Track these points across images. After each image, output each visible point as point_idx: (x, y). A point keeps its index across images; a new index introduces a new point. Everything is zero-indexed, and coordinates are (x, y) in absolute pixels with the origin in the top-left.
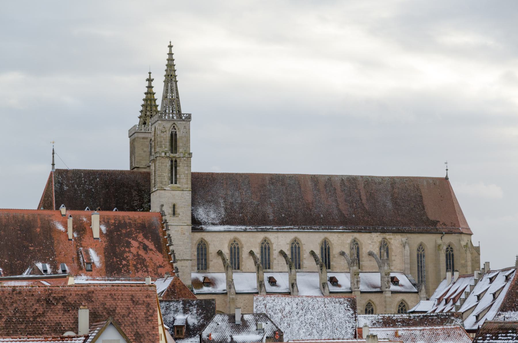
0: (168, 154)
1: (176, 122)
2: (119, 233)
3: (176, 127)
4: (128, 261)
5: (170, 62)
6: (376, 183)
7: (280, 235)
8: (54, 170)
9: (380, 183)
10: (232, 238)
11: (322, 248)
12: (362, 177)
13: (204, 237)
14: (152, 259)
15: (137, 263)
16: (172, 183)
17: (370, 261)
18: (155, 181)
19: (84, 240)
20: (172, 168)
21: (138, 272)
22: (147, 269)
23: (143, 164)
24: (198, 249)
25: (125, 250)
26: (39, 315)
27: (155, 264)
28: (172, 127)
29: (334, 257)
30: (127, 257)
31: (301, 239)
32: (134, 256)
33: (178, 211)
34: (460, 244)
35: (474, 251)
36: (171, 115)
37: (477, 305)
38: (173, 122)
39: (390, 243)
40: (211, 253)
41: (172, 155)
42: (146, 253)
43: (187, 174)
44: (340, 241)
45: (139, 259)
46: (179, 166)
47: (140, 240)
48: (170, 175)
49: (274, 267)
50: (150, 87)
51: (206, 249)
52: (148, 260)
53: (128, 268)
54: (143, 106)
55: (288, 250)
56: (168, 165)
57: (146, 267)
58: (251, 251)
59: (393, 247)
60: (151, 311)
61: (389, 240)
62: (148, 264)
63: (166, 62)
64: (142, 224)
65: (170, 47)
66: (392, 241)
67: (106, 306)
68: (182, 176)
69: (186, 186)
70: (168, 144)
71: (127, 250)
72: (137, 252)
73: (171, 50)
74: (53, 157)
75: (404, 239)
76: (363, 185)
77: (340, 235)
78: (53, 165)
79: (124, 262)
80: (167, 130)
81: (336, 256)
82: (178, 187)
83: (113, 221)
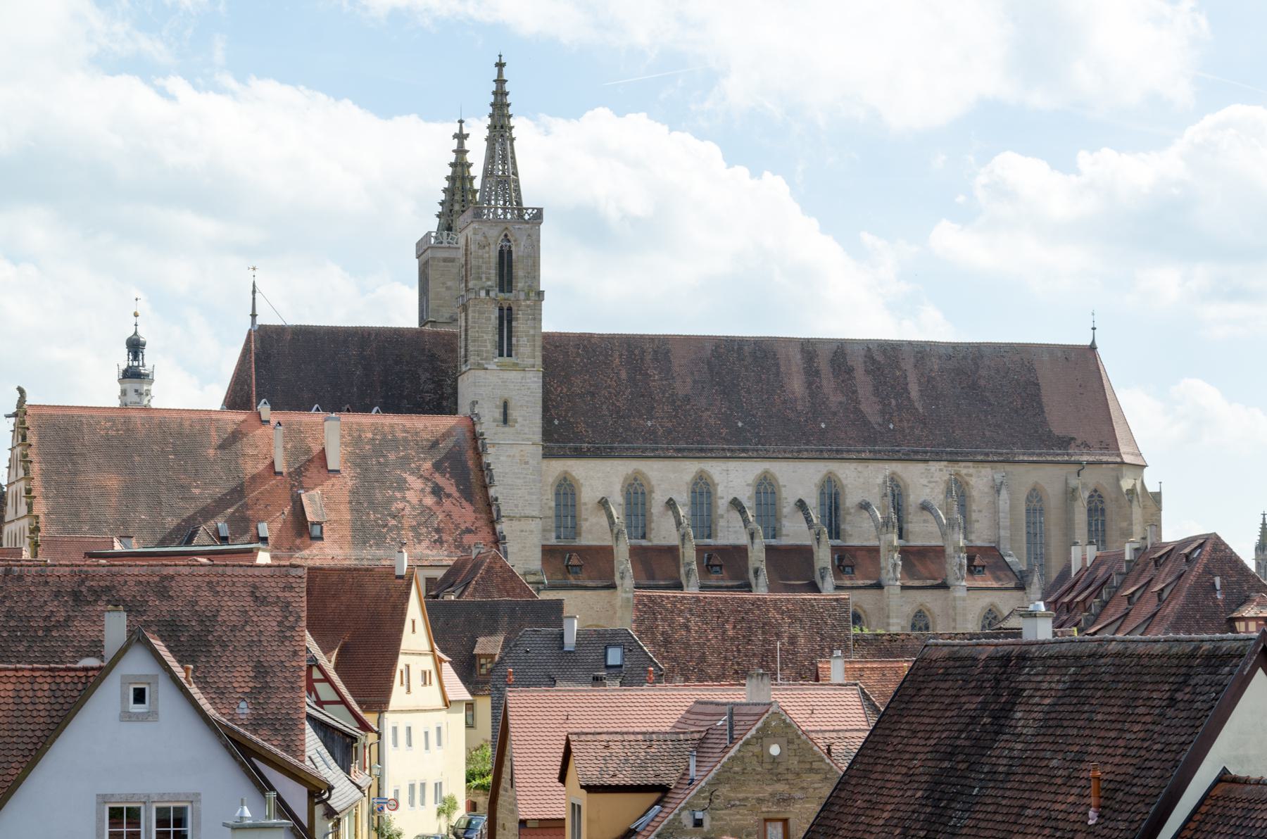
0: (492, 294)
2: (382, 460)
7: (732, 465)
9: (950, 358)
11: (822, 493)
12: (910, 343)
16: (501, 355)
17: (925, 521)
18: (466, 350)
19: (308, 474)
21: (420, 542)
23: (445, 314)
24: (557, 494)
26: (58, 625)
27: (457, 526)
29: (850, 514)
31: (778, 475)
32: (413, 508)
33: (514, 413)
34: (1119, 487)
35: (1150, 503)
36: (500, 211)
37: (1127, 614)
38: (504, 226)
39: (967, 484)
44: (862, 480)
46: (517, 319)
50: (461, 151)
51: (573, 494)
53: (399, 534)
54: (445, 191)
56: (493, 317)
58: (671, 499)
59: (975, 493)
60: (291, 619)
61: (967, 479)
63: (492, 99)
65: (500, 65)
66: (972, 481)
67: (197, 608)
68: (524, 340)
69: (531, 361)
70: (493, 272)
71: (398, 495)
72: (421, 501)
73: (500, 73)
75: (998, 477)
76: (912, 360)
77: (860, 466)
78: (254, 316)
80: (491, 241)
82: (517, 364)
83: (370, 435)
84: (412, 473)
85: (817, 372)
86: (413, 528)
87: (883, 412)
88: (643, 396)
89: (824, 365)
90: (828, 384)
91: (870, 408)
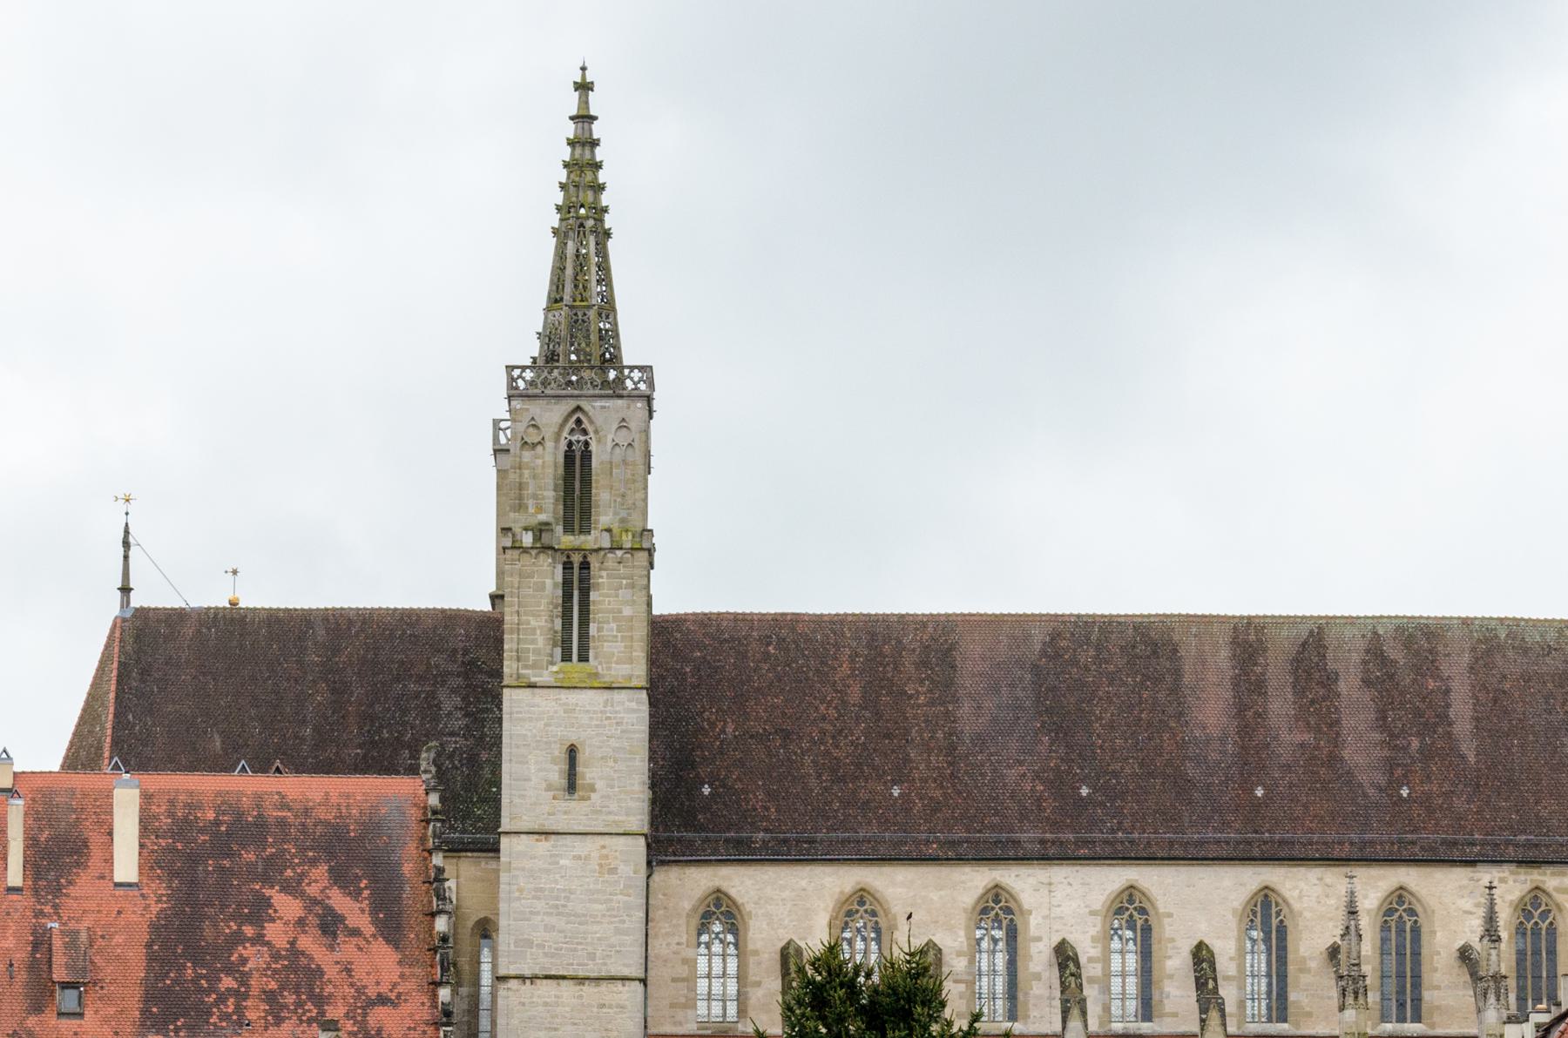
1: (584, 404)
3: (586, 424)
4: (244, 979)
5: (578, 150)
6: (1525, 651)
7: (1061, 874)
8: (128, 615)
10: (848, 889)
12: (1466, 622)
13: (725, 886)
14: (349, 971)
15: (282, 988)
19: (73, 891)
20: (567, 597)
21: (279, 1021)
22: (322, 1013)
25: (239, 932)
27: (360, 991)
28: (571, 424)
30: (244, 961)
32: (276, 956)
33: (587, 773)
38: (572, 404)
40: (756, 953)
41: (567, 541)
42: (331, 948)
43: (631, 619)
45: (293, 968)
47: (313, 890)
48: (558, 624)
49: (1034, 1013)
52: (331, 972)
55: (1094, 939)
56: (549, 582)
57: (320, 1001)
61: (1559, 897)
62: (329, 989)
64: (336, 827)
65: (584, 87)
71: (249, 931)
73: (584, 102)
74: (126, 557)
76: (1467, 658)
78: (126, 590)
79: (228, 982)
80: (548, 433)
81: (1313, 965)
83: (211, 815)
84: (283, 890)
85: (1259, 687)
86: (270, 997)
87: (1390, 765)
88: (887, 736)
89: (1276, 670)
90: (1280, 706)
91: (1361, 750)
